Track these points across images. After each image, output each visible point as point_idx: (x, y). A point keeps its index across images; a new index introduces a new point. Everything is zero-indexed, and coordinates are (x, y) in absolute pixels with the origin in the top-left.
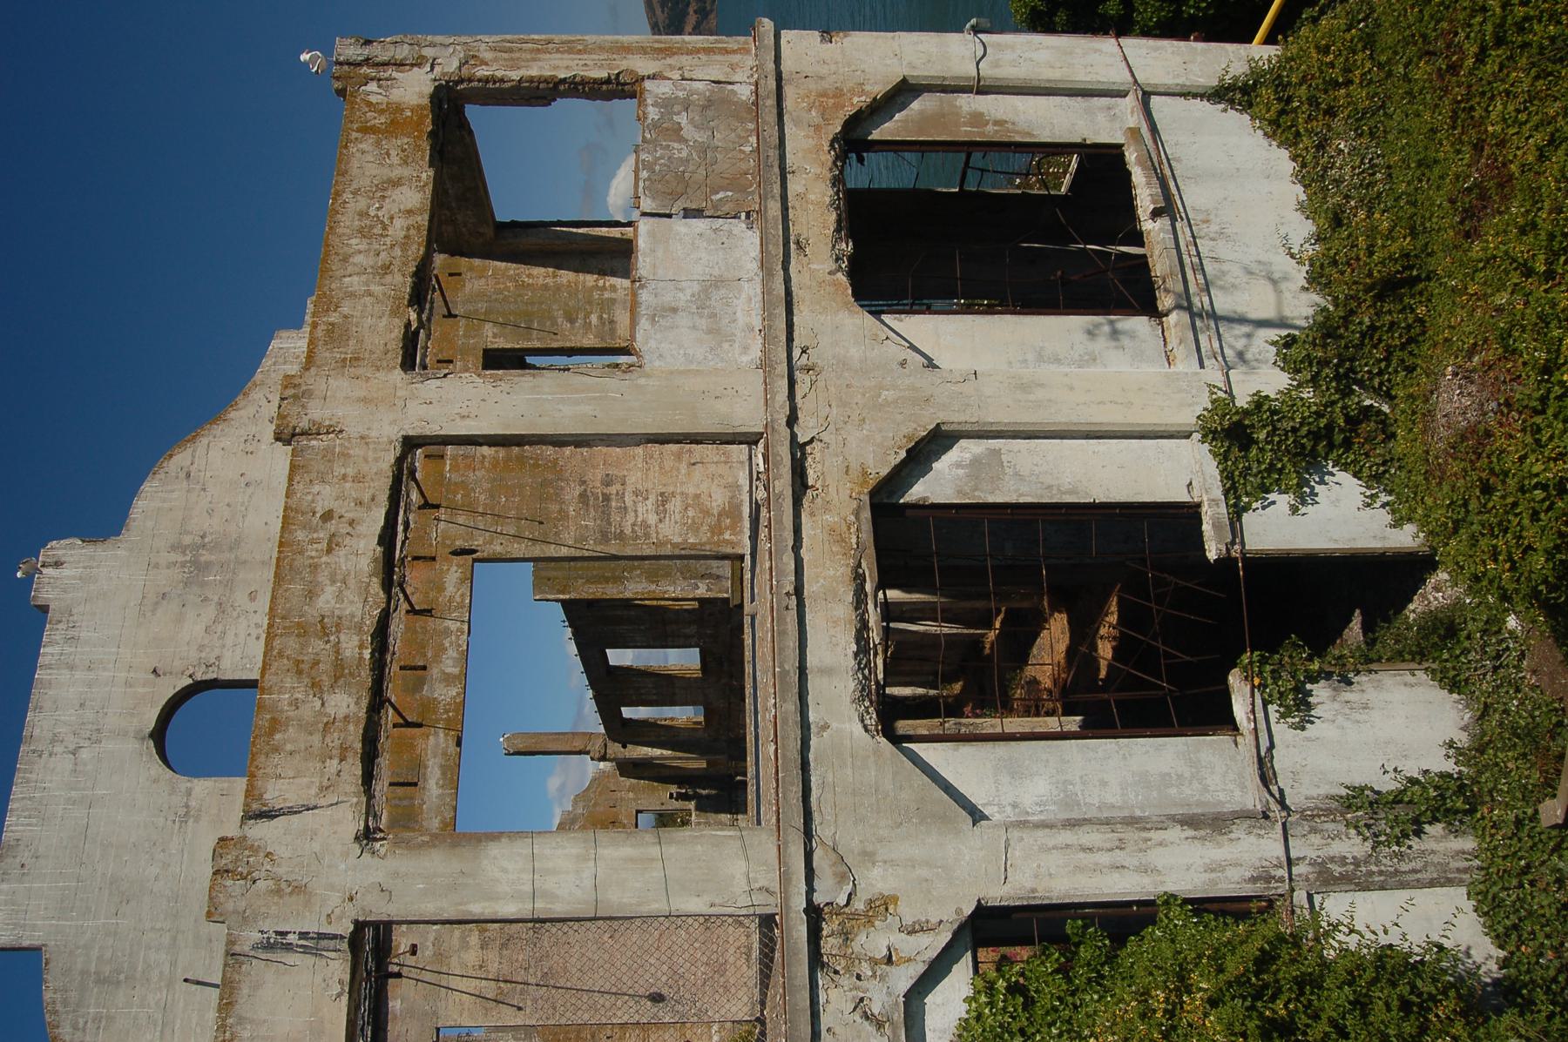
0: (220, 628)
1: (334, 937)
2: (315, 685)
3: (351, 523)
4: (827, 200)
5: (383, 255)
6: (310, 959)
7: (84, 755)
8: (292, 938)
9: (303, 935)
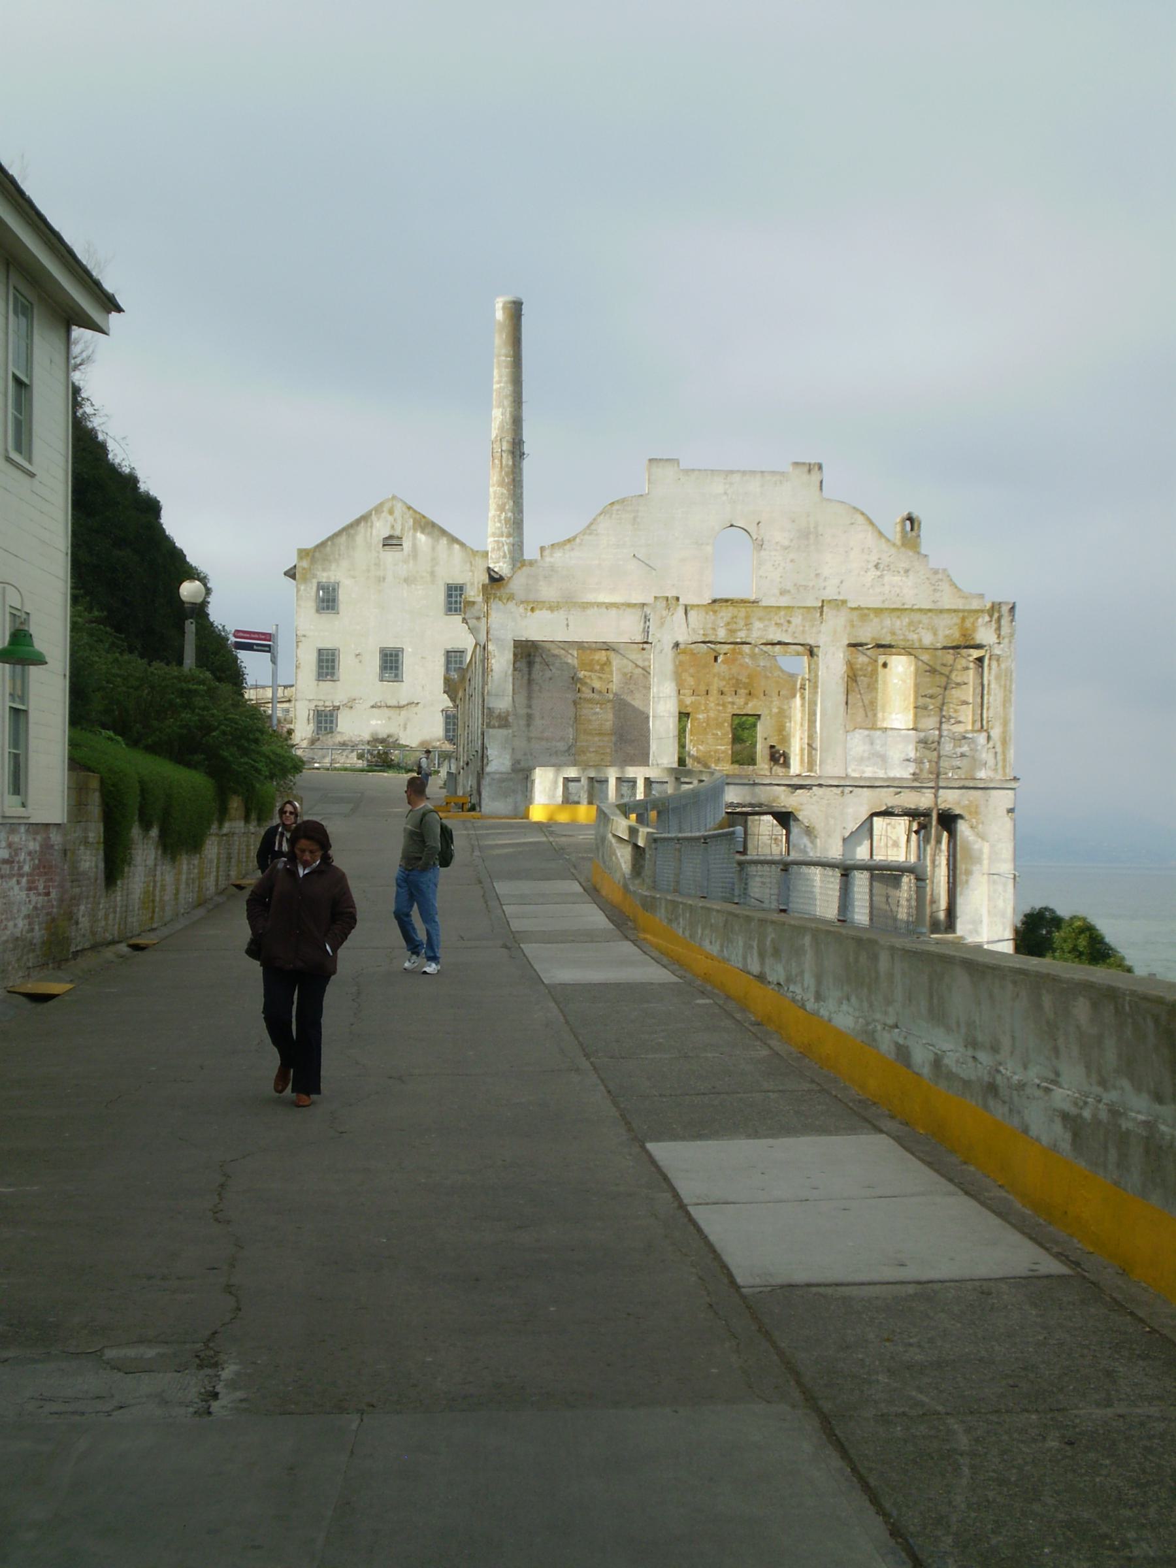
0: (779, 548)
1: (648, 636)
2: (728, 624)
3: (786, 631)
4: (921, 805)
5: (901, 632)
6: (641, 630)
7: (725, 498)
8: (648, 623)
9: (648, 627)
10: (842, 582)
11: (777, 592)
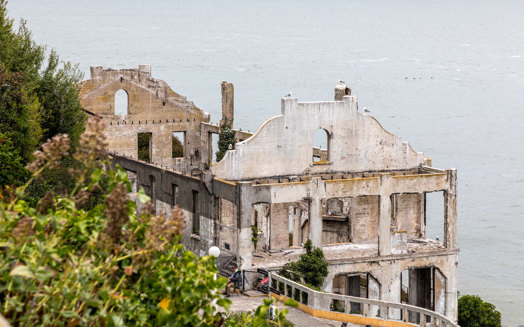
10: (366, 152)
11: (340, 158)
